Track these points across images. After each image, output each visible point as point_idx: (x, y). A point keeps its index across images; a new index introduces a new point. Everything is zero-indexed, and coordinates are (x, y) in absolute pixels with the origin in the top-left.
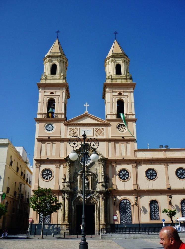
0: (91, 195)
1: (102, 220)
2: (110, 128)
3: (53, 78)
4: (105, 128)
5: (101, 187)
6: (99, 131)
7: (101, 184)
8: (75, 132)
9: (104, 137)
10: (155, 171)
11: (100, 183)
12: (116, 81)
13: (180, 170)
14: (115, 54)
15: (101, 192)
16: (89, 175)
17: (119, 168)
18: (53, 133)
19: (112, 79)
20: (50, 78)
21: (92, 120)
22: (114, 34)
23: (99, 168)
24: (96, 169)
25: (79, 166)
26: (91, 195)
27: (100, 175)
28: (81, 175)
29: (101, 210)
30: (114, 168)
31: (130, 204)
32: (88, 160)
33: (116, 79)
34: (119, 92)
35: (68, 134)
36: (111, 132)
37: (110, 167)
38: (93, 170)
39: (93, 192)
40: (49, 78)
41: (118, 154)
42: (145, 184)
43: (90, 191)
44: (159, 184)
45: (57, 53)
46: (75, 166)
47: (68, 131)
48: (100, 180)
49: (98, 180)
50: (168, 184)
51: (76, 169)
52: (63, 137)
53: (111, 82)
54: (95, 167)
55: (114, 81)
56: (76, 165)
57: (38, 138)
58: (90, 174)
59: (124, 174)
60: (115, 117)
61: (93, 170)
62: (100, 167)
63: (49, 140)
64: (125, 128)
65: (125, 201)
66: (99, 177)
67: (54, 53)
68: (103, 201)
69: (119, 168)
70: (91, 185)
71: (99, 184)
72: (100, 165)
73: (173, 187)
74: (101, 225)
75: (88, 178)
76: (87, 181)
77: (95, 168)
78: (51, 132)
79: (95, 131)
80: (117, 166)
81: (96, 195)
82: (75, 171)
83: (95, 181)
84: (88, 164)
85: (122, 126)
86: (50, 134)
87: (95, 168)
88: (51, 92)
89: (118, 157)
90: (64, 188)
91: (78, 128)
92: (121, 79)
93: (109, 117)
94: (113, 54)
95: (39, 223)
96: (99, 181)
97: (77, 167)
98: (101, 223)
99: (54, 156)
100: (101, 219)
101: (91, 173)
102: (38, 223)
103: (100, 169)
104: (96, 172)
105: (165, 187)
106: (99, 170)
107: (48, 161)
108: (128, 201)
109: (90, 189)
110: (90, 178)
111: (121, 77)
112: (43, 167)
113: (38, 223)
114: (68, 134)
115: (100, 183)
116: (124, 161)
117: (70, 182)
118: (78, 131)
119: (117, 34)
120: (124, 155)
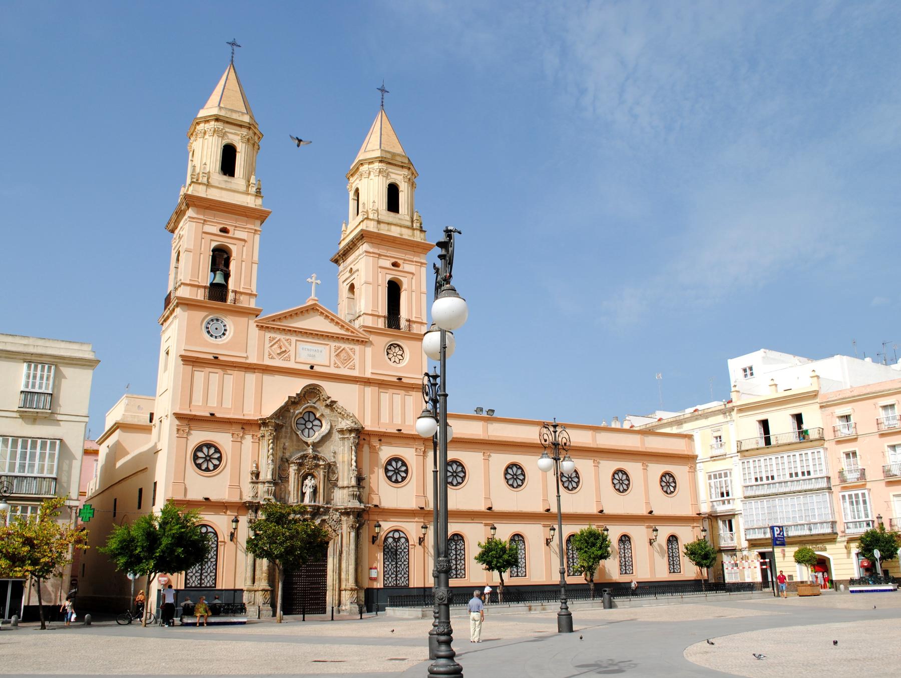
0: (324, 517)
1: (347, 580)
2: (369, 350)
4: (357, 348)
5: (346, 498)
6: (343, 355)
7: (346, 491)
8: (283, 349)
10: (463, 467)
11: (343, 488)
15: (346, 513)
16: (317, 466)
17: (386, 452)
21: (327, 321)
23: (343, 450)
24: (335, 453)
25: (292, 441)
26: (324, 517)
27: (346, 467)
28: (300, 465)
29: (344, 554)
30: (374, 451)
32: (315, 428)
35: (266, 354)
36: (369, 360)
37: (366, 449)
38: (326, 452)
39: (327, 511)
41: (385, 419)
43: (319, 507)
46: (283, 440)
47: (267, 345)
48: (343, 481)
49: (337, 480)
51: (284, 449)
54: (332, 447)
56: (286, 437)
58: (321, 463)
61: (326, 452)
62: (346, 449)
66: (340, 474)
68: (353, 534)
69: (386, 452)
70: (321, 491)
71: (341, 491)
72: (344, 446)
74: (345, 590)
75: (316, 474)
77: (332, 448)
79: (333, 354)
80: (382, 448)
81: (335, 517)
83: (331, 483)
84: (316, 437)
85: (397, 349)
87: (332, 448)
89: (386, 425)
90: (256, 496)
91: (293, 338)
96: (340, 484)
98: (343, 587)
100: (343, 576)
101: (324, 461)
102: (183, 588)
103: (343, 454)
104: (333, 460)
106: (341, 453)
109: (320, 502)
110: (320, 474)
113: (183, 588)
114: (266, 354)
115: (343, 488)
116: (399, 437)
117: (274, 482)
118: (292, 349)
120: (398, 422)
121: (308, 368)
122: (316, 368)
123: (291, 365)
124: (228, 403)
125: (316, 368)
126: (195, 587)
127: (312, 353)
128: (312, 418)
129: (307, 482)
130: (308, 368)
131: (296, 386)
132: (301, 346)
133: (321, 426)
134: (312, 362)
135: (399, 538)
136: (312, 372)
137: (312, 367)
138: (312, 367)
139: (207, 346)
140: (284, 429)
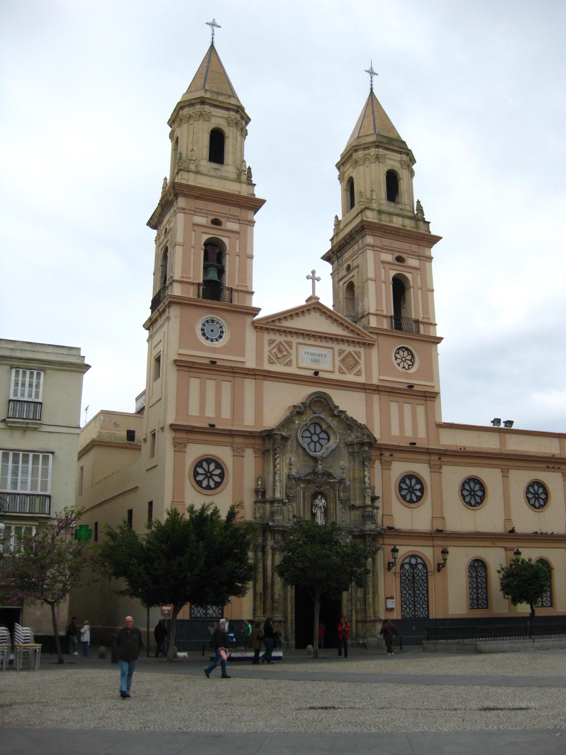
3: (218, 173)
9: (361, 379)
12: (390, 221)
13: (539, 487)
14: (385, 140)
18: (222, 350)
19: (380, 212)
20: (208, 171)
22: (368, 75)
31: (425, 566)
33: (390, 214)
34: (397, 254)
40: (206, 172)
42: (459, 519)
44: (488, 519)
45: (225, 95)
46: (288, 455)
50: (508, 520)
52: (251, 364)
53: (376, 221)
55: (385, 220)
56: (292, 451)
57: (177, 357)
59: (205, 474)
60: (386, 324)
63: (213, 367)
64: (410, 360)
67: (218, 93)
73: (520, 529)
76: (323, 501)
78: (216, 344)
82: (290, 469)
86: (214, 350)
88: (213, 217)
92: (403, 216)
93: (373, 322)
94: (380, 139)
95: (191, 617)
97: (293, 459)
99: (225, 418)
105: (498, 527)
107: (211, 432)
108: (419, 561)
111: (401, 209)
112: (196, 451)
119: (375, 77)
121: (311, 373)
122: (321, 374)
125: (321, 374)
126: (201, 617)
127: (315, 357)
128: (318, 430)
129: (317, 501)
130: (311, 373)
131: (300, 394)
132: (303, 350)
133: (329, 439)
134: (316, 367)
136: (315, 378)
137: (316, 373)
138: (316, 373)
140: (289, 443)
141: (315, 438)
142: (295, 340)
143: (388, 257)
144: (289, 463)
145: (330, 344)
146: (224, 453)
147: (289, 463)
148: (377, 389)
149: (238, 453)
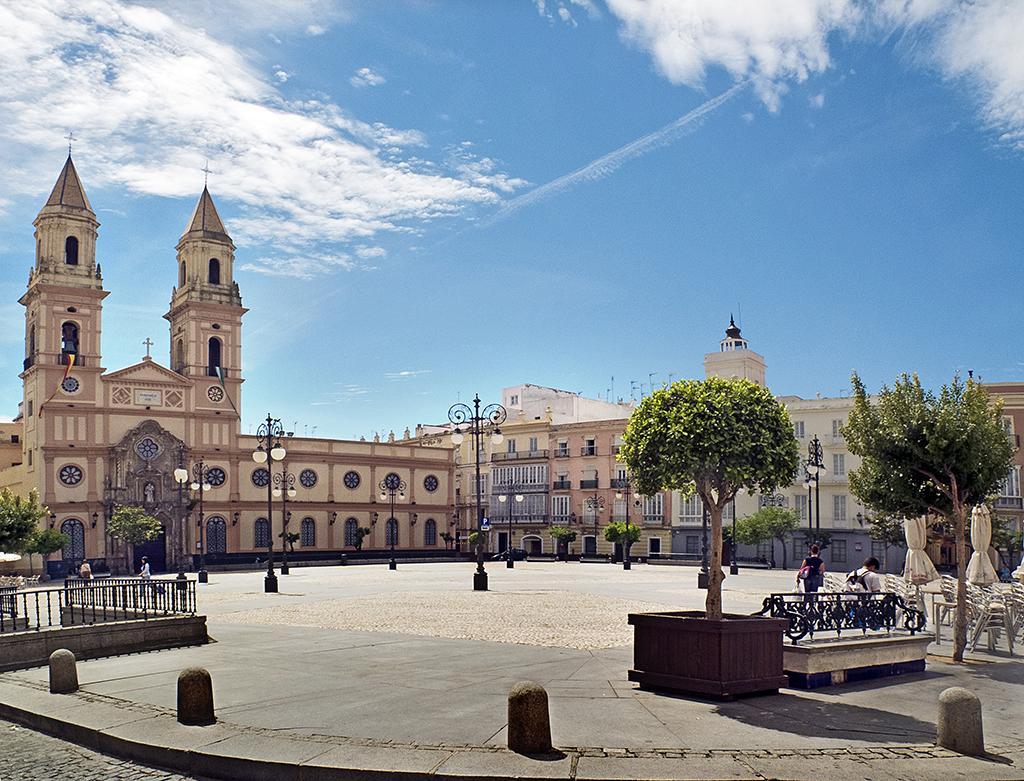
9: (183, 409)
18: (81, 397)
31: (224, 523)
52: (99, 403)
65: (216, 520)
86: (72, 398)
107: (71, 449)
112: (60, 462)
123: (131, 406)
124: (82, 437)
134: (148, 403)
135: (218, 522)
137: (148, 408)
138: (148, 408)
139: (65, 398)
141: (147, 448)
142: (132, 387)
143: (207, 325)
144: (127, 465)
145: (159, 388)
146: (82, 462)
147: (127, 465)
148: (194, 416)
149: (92, 461)
